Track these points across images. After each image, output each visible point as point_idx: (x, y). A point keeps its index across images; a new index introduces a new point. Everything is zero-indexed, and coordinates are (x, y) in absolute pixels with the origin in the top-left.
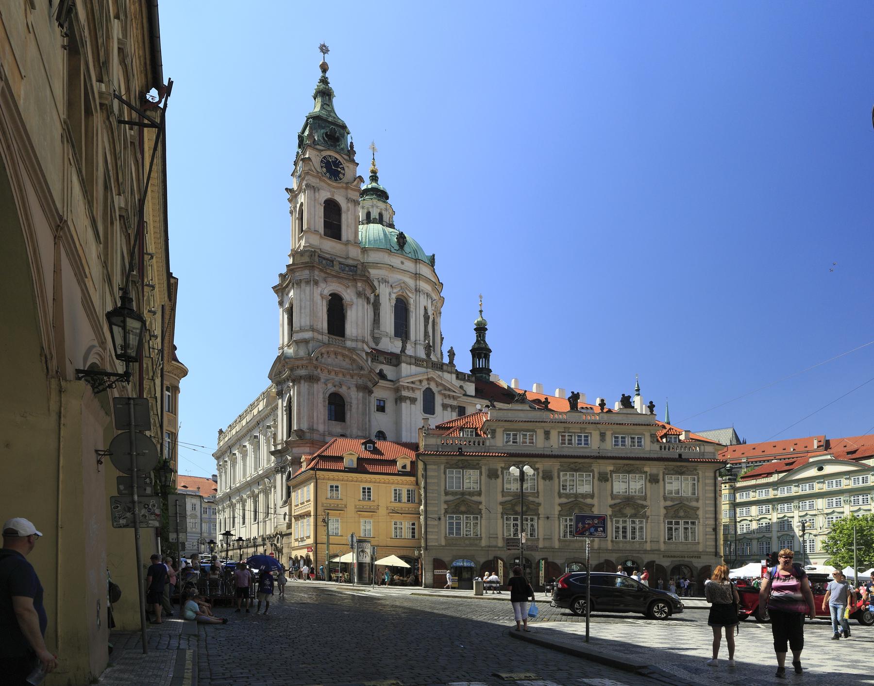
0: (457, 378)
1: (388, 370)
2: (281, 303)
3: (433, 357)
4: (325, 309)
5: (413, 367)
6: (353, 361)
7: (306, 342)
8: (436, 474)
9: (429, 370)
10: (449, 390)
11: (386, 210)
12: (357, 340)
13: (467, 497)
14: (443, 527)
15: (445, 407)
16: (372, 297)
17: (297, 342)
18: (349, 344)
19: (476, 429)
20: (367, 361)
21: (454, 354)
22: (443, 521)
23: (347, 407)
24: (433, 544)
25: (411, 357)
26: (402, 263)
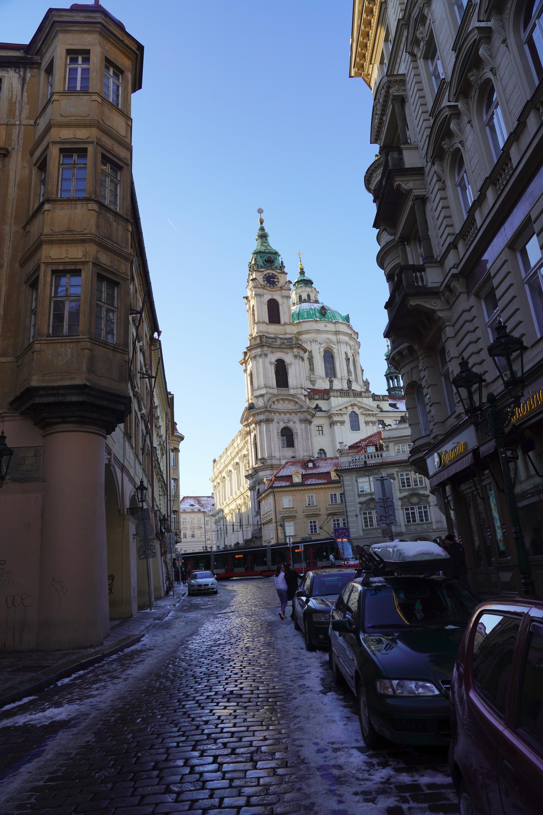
0: (374, 400)
1: (322, 404)
2: (245, 371)
4: (273, 371)
5: (340, 398)
6: (296, 403)
7: (262, 396)
8: (351, 482)
10: (368, 410)
11: (312, 291)
12: (297, 388)
14: (360, 521)
15: (367, 423)
16: (306, 356)
17: (257, 397)
18: (292, 392)
20: (305, 402)
21: (369, 384)
22: (359, 516)
24: (354, 536)
26: (326, 326)
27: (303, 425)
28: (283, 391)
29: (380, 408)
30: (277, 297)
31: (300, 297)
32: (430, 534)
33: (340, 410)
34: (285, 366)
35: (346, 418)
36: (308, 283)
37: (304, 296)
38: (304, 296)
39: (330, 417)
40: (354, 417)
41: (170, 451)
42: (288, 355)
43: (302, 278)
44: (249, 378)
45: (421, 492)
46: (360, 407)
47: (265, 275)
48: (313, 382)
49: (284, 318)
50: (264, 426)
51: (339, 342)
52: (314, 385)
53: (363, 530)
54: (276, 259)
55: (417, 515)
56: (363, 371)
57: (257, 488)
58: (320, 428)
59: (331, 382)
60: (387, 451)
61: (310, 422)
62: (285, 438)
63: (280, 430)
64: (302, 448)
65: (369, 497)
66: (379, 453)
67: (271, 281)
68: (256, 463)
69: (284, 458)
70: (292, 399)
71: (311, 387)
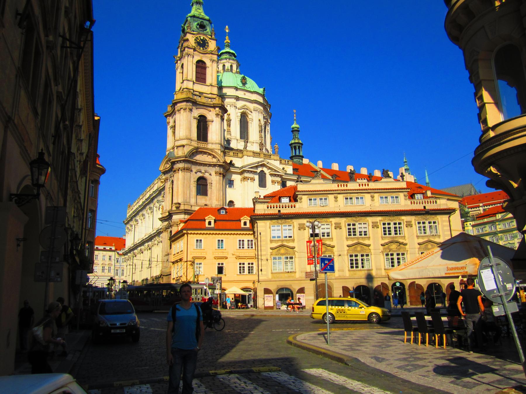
0: (281, 163)
10: (275, 171)
13: (285, 243)
15: (273, 182)
17: (178, 147)
18: (210, 146)
25: (250, 151)
26: (245, 94)
27: (218, 177)
28: (202, 145)
29: (286, 171)
30: (207, 59)
31: (224, 66)
33: (251, 168)
35: (257, 177)
37: (228, 66)
38: (228, 66)
41: (90, 182)
42: (210, 113)
46: (270, 168)
47: (197, 38)
53: (272, 273)
59: (246, 142)
60: (301, 202)
63: (196, 179)
64: (215, 198)
65: (280, 244)
66: (293, 204)
71: (227, 146)
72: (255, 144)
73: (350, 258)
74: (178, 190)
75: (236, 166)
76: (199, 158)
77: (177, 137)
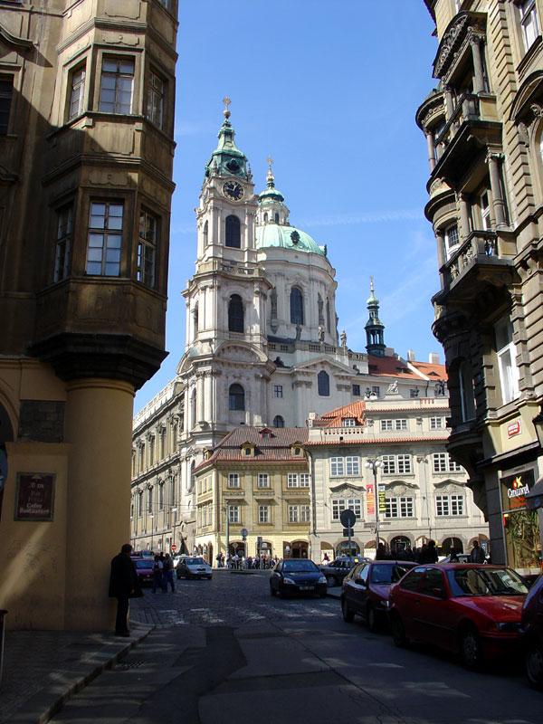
1: (285, 358)
3: (327, 339)
4: (227, 310)
7: (210, 341)
9: (323, 354)
10: (343, 371)
11: (282, 210)
13: (349, 482)
15: (339, 387)
16: (269, 292)
17: (203, 341)
18: (248, 341)
19: (356, 419)
23: (246, 397)
27: (259, 383)
29: (358, 370)
31: (266, 215)
32: (412, 532)
34: (242, 304)
35: (315, 381)
36: (278, 198)
39: (293, 375)
40: (323, 378)
42: (247, 291)
43: (270, 191)
44: (192, 315)
45: (407, 481)
48: (274, 329)
49: (245, 243)
50: (208, 380)
51: (312, 279)
52: (275, 332)
54: (242, 165)
55: (399, 508)
56: (337, 319)
57: (192, 459)
58: (279, 391)
61: (267, 380)
62: (234, 397)
63: (229, 385)
67: (235, 192)
68: (194, 427)
69: (231, 423)
70: (247, 348)
71: (272, 334)
72: (313, 330)
73: (437, 501)
74: (203, 403)
75: (285, 365)
76: (232, 355)
77: (201, 327)
